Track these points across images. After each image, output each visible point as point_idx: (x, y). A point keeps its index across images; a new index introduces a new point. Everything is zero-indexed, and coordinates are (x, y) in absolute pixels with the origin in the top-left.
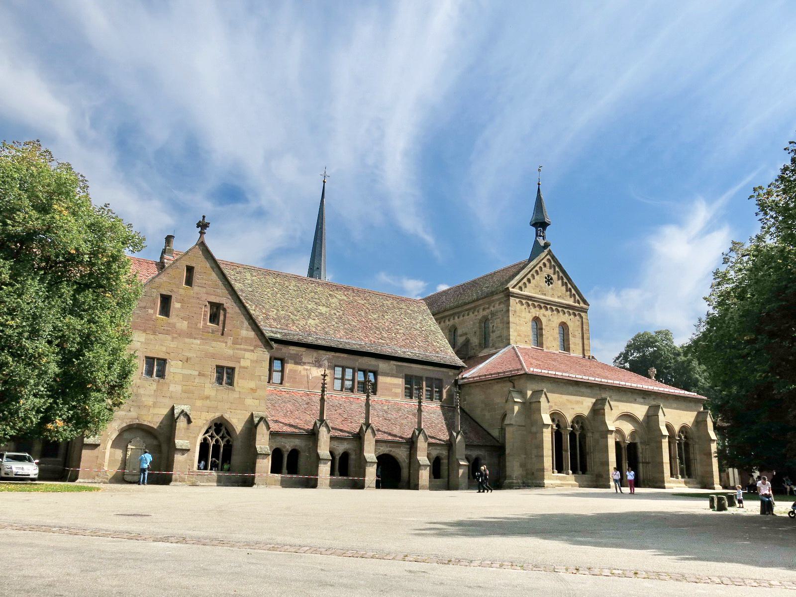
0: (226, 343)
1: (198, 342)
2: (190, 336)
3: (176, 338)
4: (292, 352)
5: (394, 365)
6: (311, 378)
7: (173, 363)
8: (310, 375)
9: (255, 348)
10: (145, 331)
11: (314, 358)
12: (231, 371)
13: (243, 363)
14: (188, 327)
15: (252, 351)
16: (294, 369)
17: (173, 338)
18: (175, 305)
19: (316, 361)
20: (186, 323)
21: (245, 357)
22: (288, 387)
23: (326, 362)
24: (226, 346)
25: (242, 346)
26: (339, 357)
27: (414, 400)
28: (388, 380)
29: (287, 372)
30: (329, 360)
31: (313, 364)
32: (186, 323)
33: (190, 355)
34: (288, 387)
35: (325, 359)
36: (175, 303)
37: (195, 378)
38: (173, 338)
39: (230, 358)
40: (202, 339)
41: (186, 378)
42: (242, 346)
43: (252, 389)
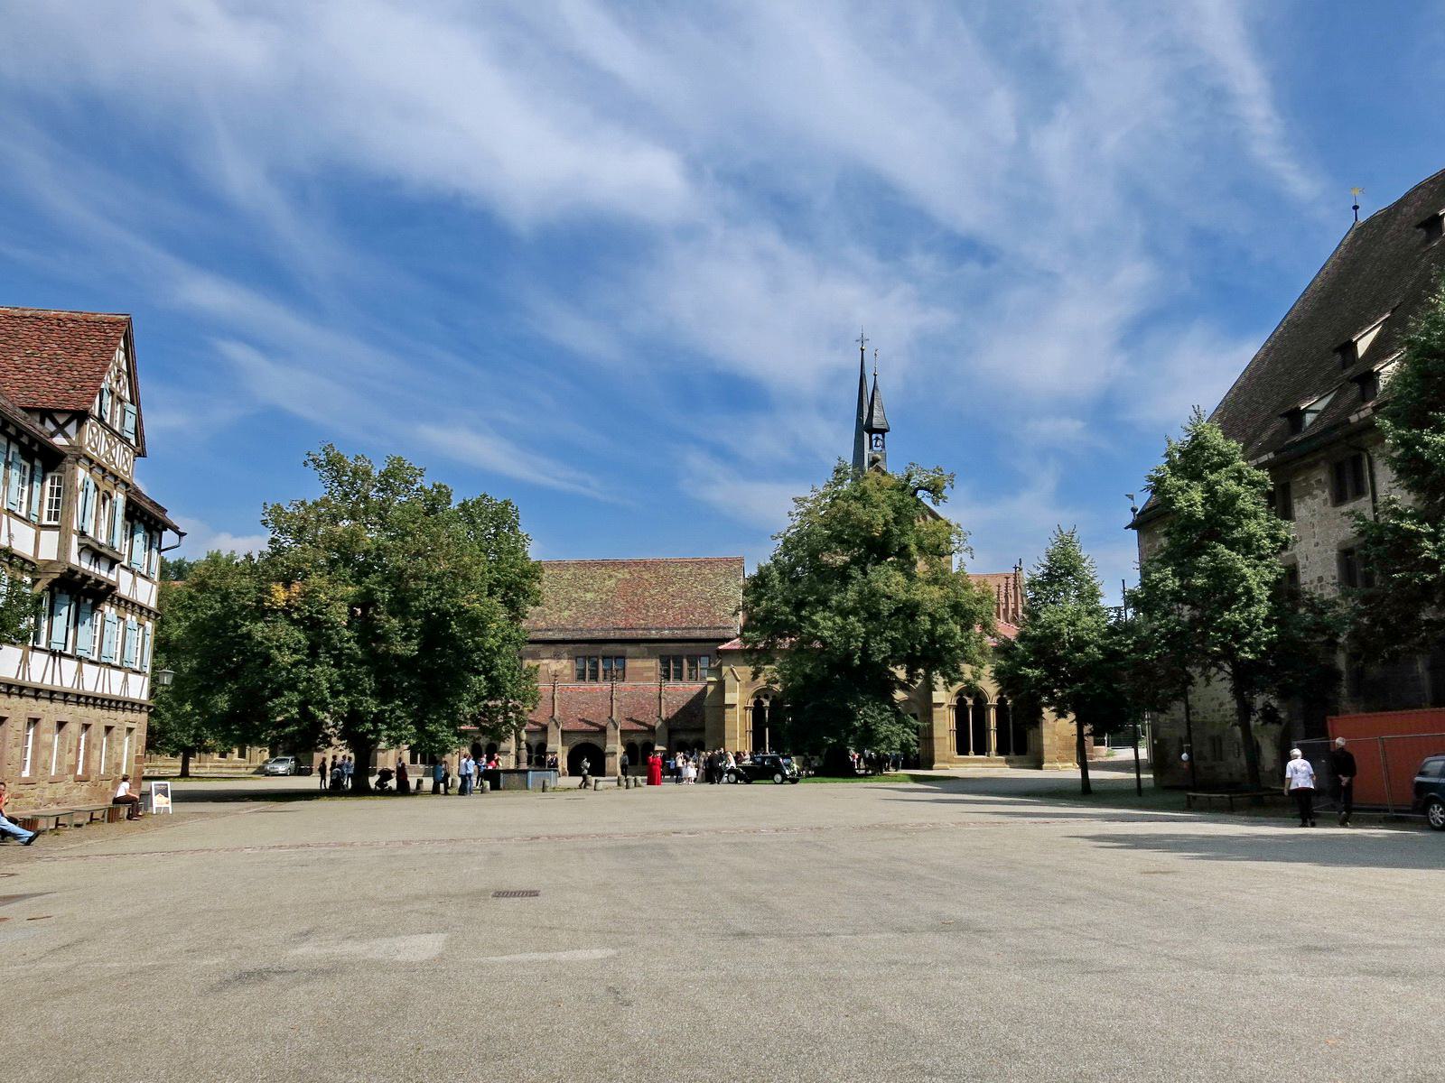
23: (566, 655)
28: (639, 664)
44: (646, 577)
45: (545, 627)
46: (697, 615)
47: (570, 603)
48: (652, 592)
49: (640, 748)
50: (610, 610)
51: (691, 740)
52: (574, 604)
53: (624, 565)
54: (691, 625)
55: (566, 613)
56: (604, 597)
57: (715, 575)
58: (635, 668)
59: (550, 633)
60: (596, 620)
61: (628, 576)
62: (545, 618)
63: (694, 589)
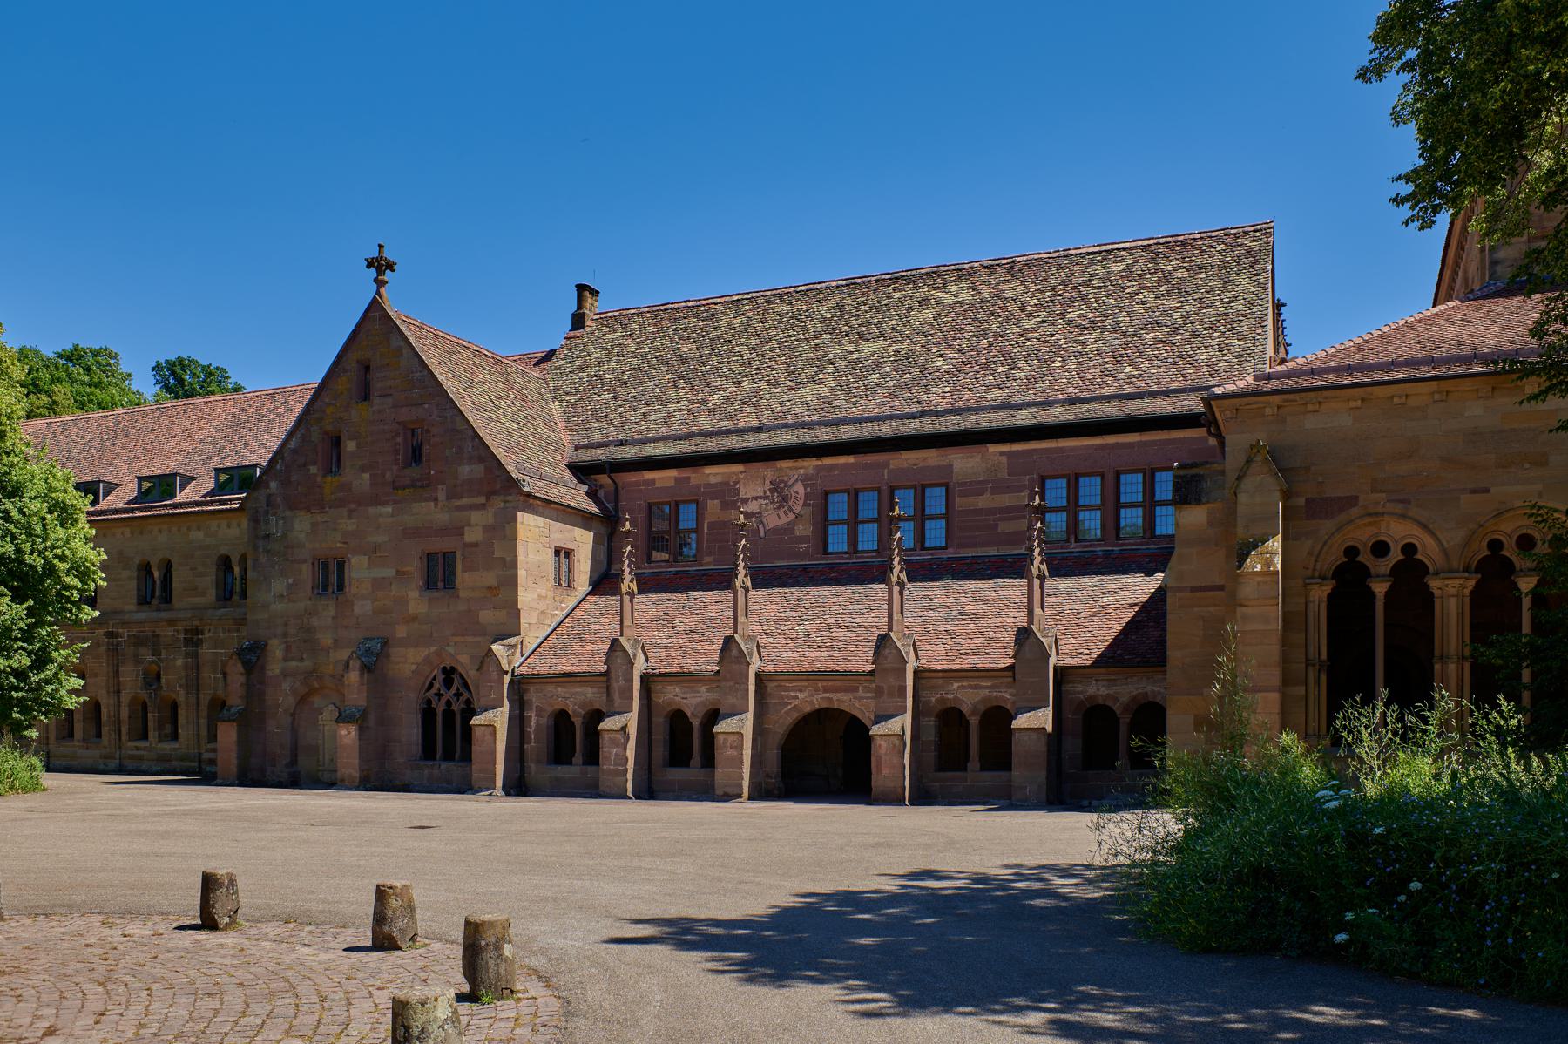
0: (436, 500)
1: (389, 509)
2: (377, 501)
3: (354, 510)
4: (713, 480)
5: (1002, 453)
6: (762, 534)
7: (354, 560)
8: (761, 526)
9: (488, 499)
10: (308, 509)
11: (768, 482)
12: (448, 558)
13: (472, 535)
14: (371, 484)
15: (483, 506)
16: (721, 519)
17: (351, 511)
18: (350, 446)
19: (769, 489)
20: (366, 476)
21: (473, 521)
22: (708, 564)
24: (436, 505)
25: (465, 501)
26: (832, 467)
27: (1074, 545)
29: (706, 530)
30: (806, 480)
31: (767, 498)
32: (366, 476)
33: (380, 538)
34: (708, 564)
35: (797, 480)
36: (348, 442)
37: (391, 584)
38: (351, 511)
39: (445, 531)
40: (395, 502)
41: (378, 584)
42: (465, 501)
43: (490, 588)
44: (1009, 294)
45: (755, 424)
46: (1145, 365)
47: (821, 368)
48: (1027, 324)
49: (974, 721)
50: (916, 373)
51: (1125, 699)
52: (830, 369)
53: (962, 273)
54: (1128, 389)
55: (811, 389)
56: (905, 348)
57: (1196, 270)
58: (978, 512)
59: (763, 435)
60: (879, 398)
61: (967, 296)
62: (757, 405)
63: (1138, 308)
